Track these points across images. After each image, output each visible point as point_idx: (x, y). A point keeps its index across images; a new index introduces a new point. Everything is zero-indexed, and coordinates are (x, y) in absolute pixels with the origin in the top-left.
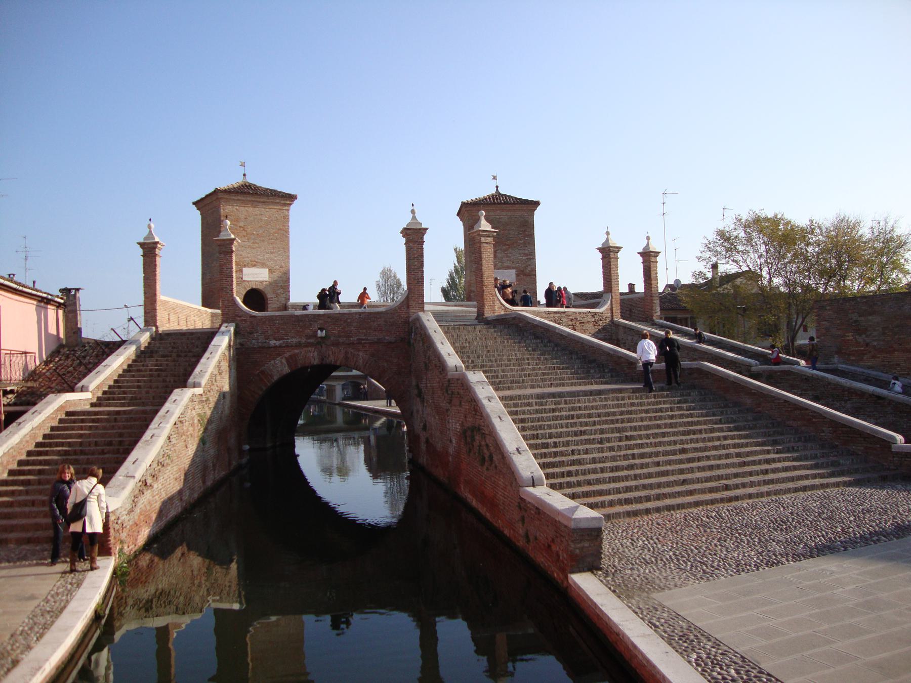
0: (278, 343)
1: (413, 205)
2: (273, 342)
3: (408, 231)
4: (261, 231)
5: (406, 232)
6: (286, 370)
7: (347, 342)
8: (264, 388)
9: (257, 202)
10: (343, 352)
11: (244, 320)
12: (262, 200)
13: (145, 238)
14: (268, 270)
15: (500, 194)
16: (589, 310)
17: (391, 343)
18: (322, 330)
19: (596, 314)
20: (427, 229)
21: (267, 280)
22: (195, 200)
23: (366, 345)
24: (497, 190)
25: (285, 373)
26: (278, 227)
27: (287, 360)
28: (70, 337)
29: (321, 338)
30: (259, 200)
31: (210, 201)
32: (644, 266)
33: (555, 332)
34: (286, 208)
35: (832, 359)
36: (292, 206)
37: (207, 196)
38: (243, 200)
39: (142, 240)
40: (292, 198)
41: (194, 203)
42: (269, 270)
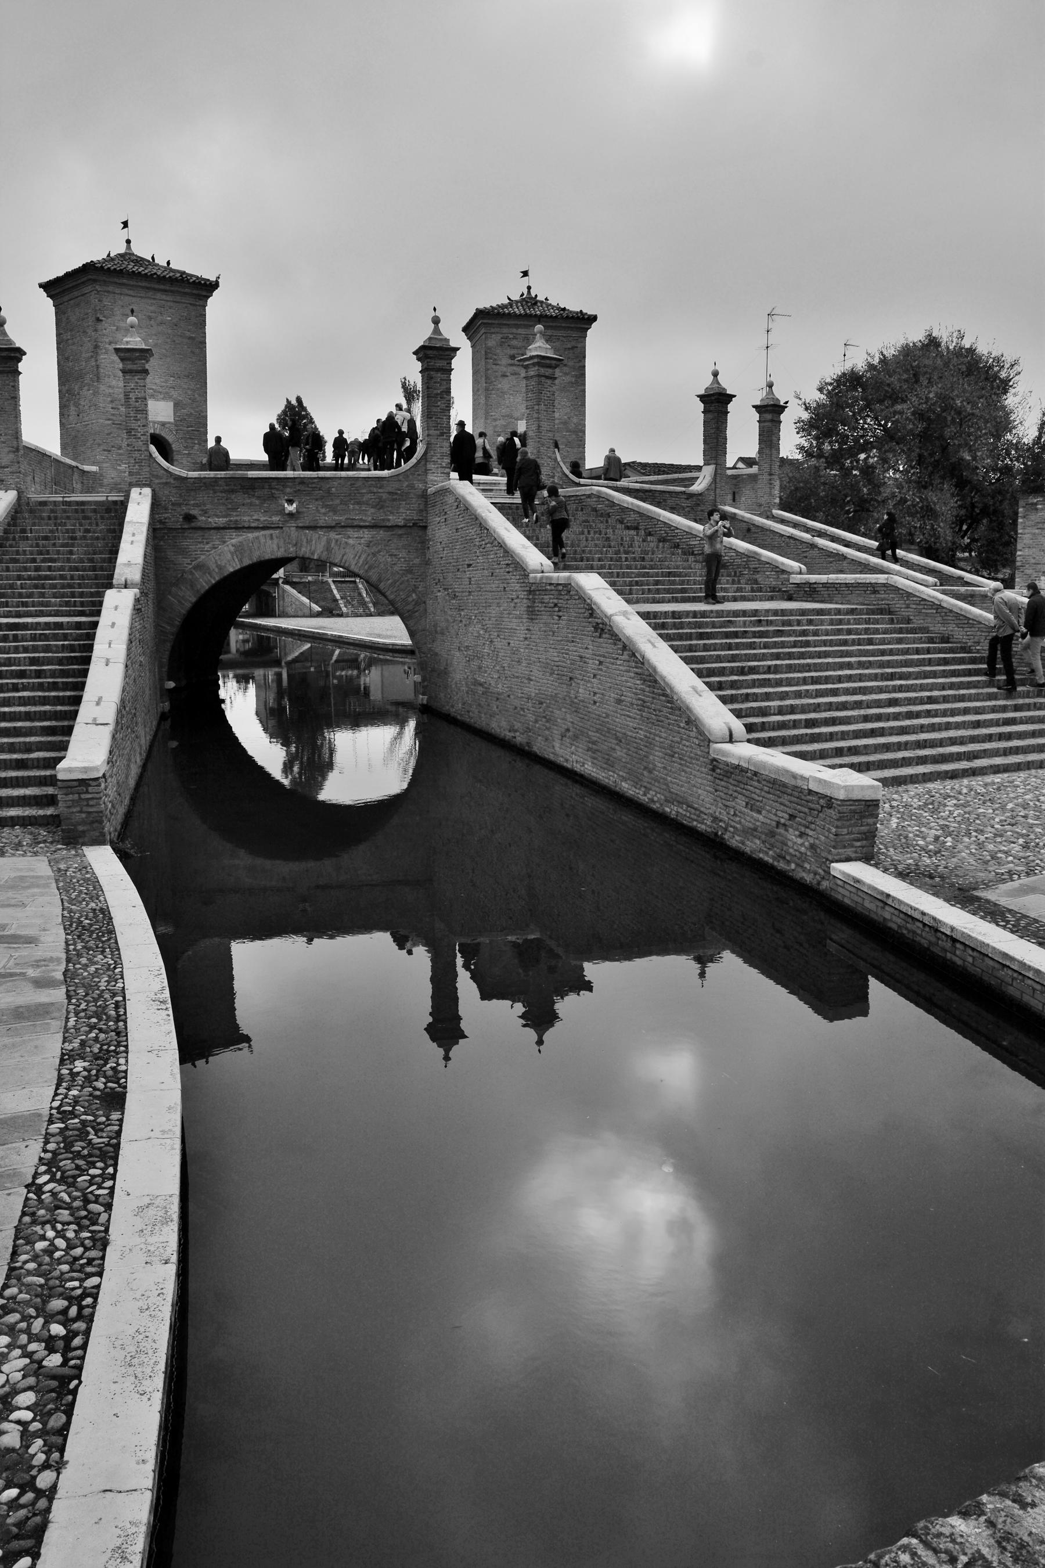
1: (435, 309)
3: (429, 352)
9: (154, 289)
11: (166, 483)
14: (171, 404)
18: (290, 502)
20: (458, 349)
21: (172, 420)
29: (291, 515)
30: (157, 286)
34: (201, 302)
36: (210, 300)
37: (68, 275)
38: (133, 286)
40: (211, 287)
42: (176, 405)
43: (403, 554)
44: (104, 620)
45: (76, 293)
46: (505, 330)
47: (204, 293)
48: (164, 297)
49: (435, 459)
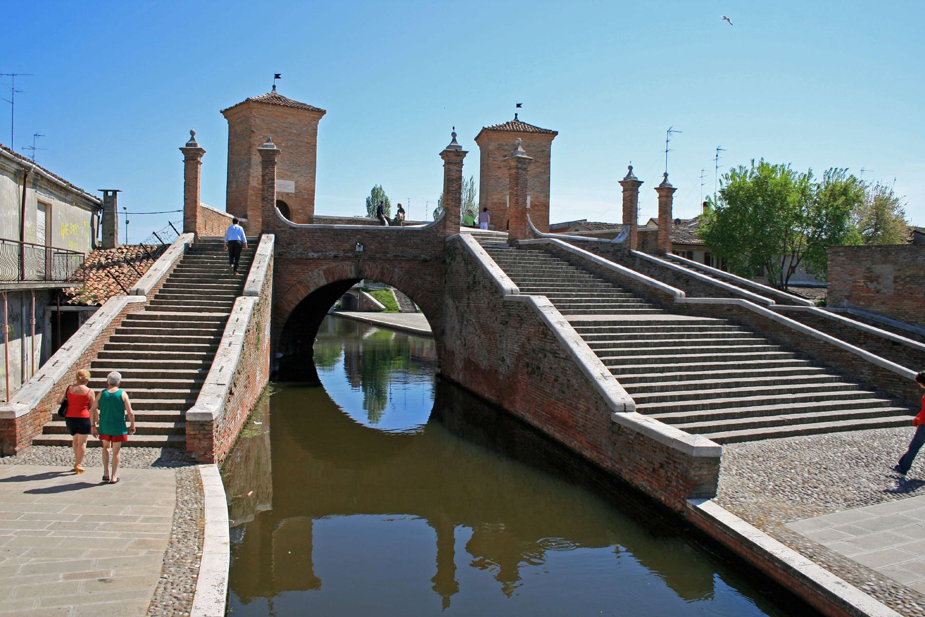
0: (316, 255)
1: (454, 128)
2: (311, 254)
4: (290, 143)
6: (323, 282)
7: (384, 257)
8: (301, 299)
10: (379, 267)
14: (294, 182)
15: (518, 121)
16: (608, 240)
19: (615, 244)
21: (293, 191)
22: (223, 109)
24: (516, 118)
25: (322, 285)
26: (306, 140)
28: (106, 238)
32: (659, 201)
33: (590, 261)
35: (841, 303)
39: (184, 146)
43: (429, 278)
44: (233, 316)
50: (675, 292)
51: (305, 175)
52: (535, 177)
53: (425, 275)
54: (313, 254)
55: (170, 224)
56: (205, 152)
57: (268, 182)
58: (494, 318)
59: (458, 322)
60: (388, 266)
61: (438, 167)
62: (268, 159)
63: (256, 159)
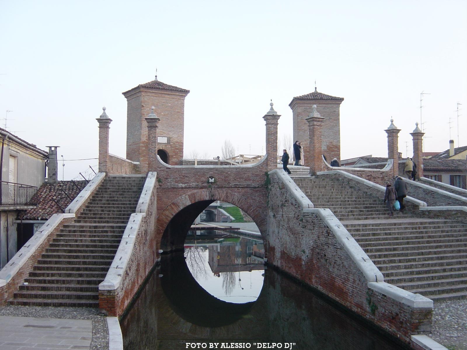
0: (183, 186)
1: (271, 100)
2: (180, 185)
3: (268, 117)
4: (167, 113)
5: (266, 117)
6: (188, 203)
7: (227, 186)
8: (174, 214)
9: (165, 94)
12: (168, 93)
13: (101, 116)
17: (255, 187)
19: (383, 172)
20: (280, 116)
23: (239, 188)
24: (316, 90)
27: (189, 196)
29: (211, 183)
30: (166, 93)
31: (135, 92)
33: (364, 184)
36: (186, 97)
37: (133, 90)
39: (99, 117)
40: (186, 92)
41: (124, 94)
43: (258, 199)
44: (129, 226)
45: (135, 96)
46: (306, 105)
47: (184, 95)
48: (168, 97)
49: (270, 160)
50: (419, 204)
51: (177, 133)
52: (330, 129)
53: (255, 197)
54: (181, 184)
55: (90, 167)
56: (112, 121)
57: (152, 139)
58: (298, 224)
59: (277, 227)
60: (231, 192)
61: (262, 126)
62: (152, 123)
63: (145, 124)
